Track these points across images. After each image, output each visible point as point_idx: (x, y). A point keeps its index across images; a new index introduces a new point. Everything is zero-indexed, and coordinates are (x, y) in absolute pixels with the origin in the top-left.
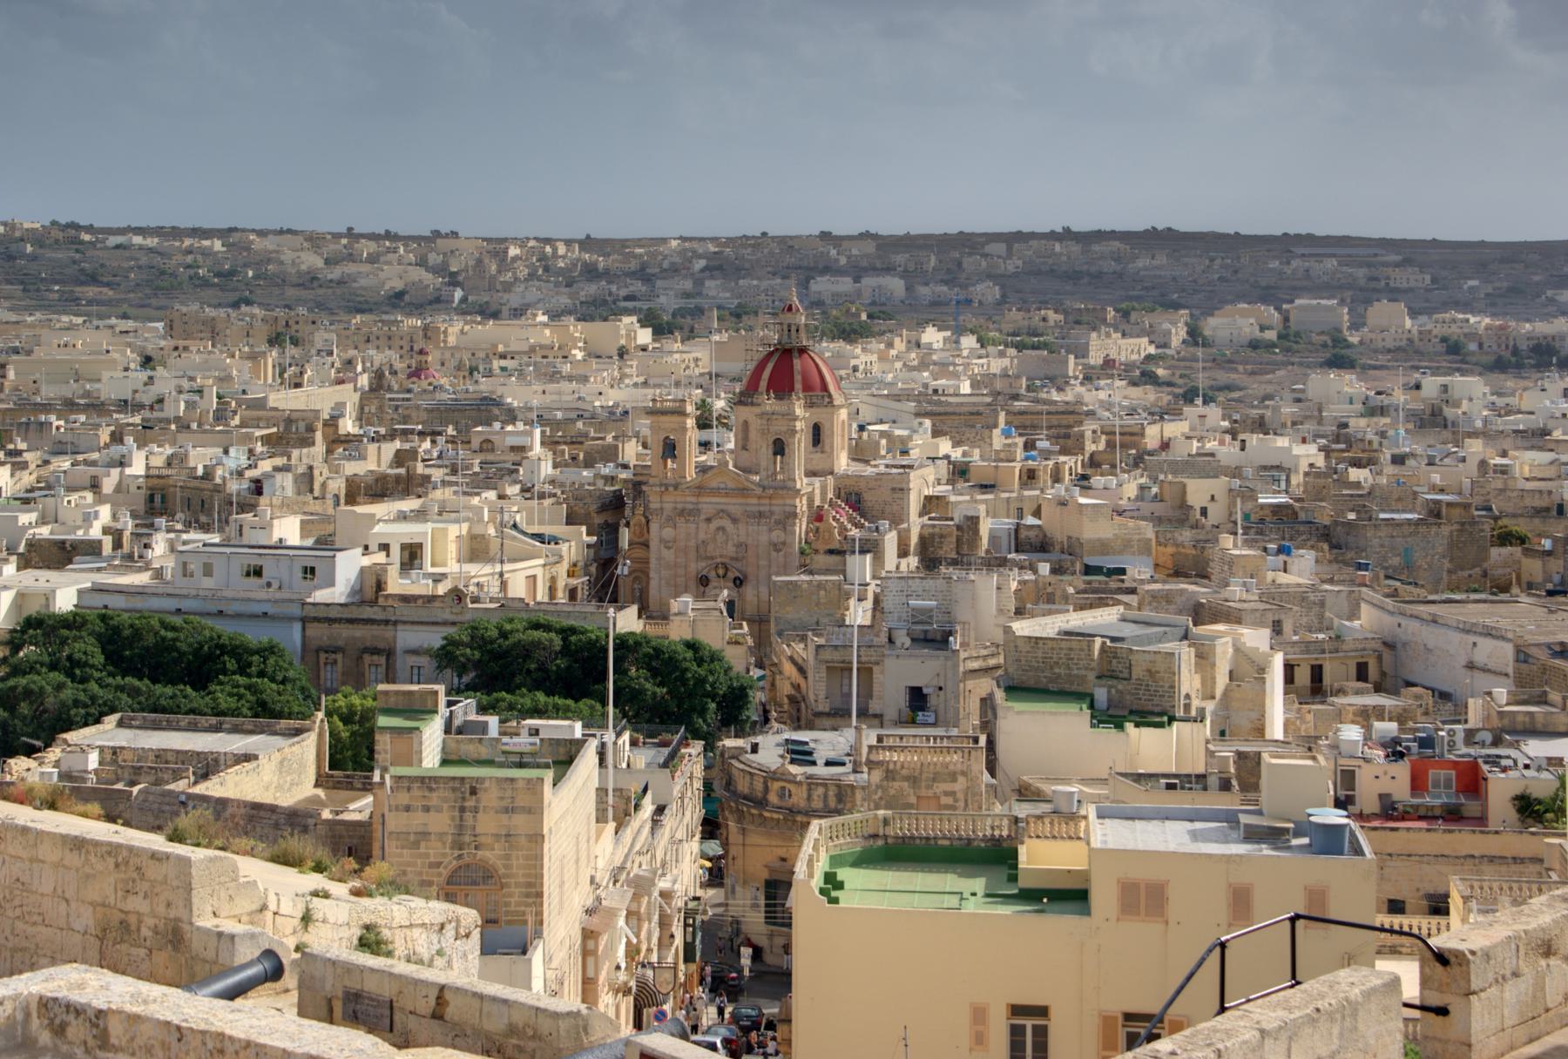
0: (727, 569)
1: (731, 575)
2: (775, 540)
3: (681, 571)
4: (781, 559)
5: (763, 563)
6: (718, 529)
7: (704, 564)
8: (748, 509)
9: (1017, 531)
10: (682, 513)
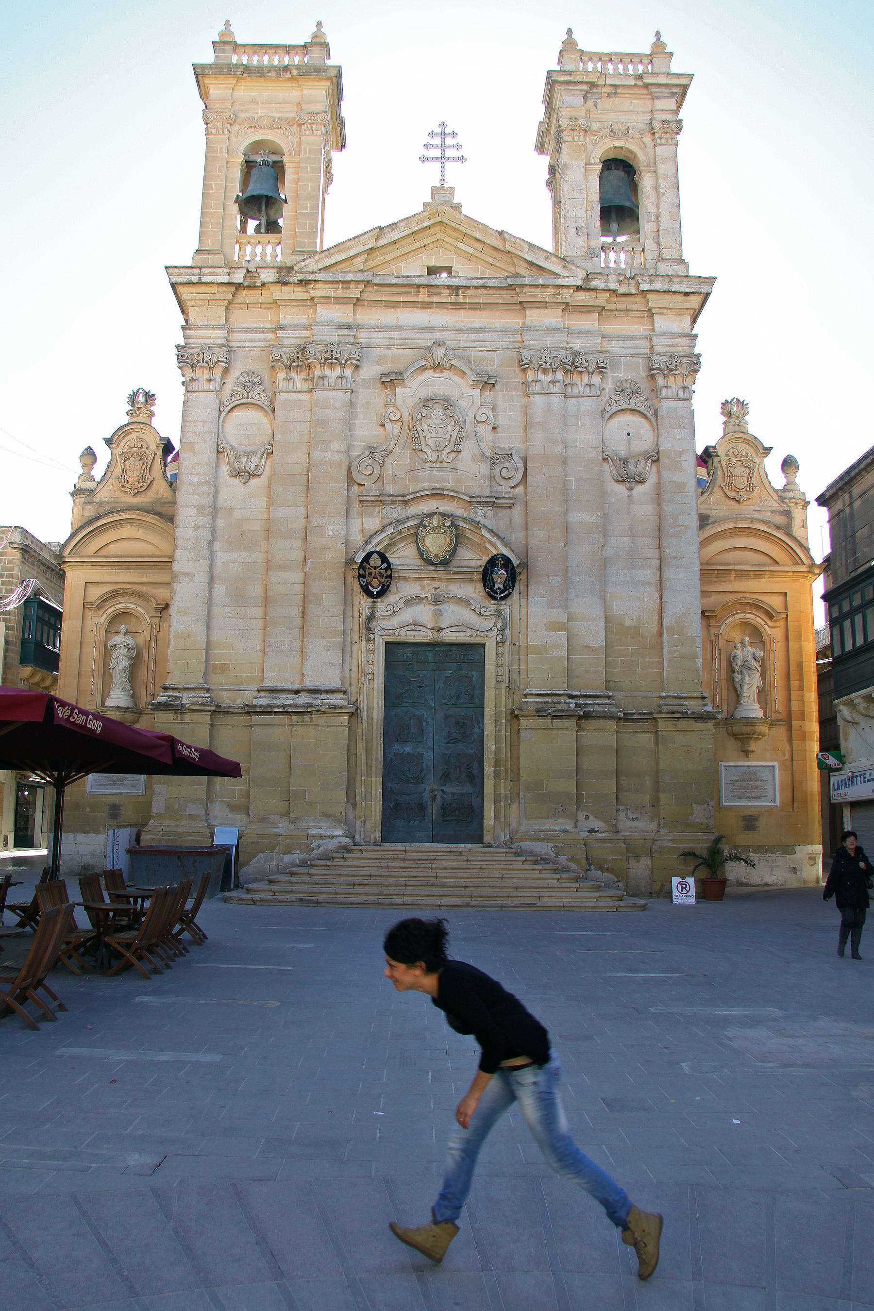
0: (458, 539)
3: (290, 550)
4: (645, 510)
5: (580, 517)
6: (427, 402)
7: (372, 523)
8: (530, 340)
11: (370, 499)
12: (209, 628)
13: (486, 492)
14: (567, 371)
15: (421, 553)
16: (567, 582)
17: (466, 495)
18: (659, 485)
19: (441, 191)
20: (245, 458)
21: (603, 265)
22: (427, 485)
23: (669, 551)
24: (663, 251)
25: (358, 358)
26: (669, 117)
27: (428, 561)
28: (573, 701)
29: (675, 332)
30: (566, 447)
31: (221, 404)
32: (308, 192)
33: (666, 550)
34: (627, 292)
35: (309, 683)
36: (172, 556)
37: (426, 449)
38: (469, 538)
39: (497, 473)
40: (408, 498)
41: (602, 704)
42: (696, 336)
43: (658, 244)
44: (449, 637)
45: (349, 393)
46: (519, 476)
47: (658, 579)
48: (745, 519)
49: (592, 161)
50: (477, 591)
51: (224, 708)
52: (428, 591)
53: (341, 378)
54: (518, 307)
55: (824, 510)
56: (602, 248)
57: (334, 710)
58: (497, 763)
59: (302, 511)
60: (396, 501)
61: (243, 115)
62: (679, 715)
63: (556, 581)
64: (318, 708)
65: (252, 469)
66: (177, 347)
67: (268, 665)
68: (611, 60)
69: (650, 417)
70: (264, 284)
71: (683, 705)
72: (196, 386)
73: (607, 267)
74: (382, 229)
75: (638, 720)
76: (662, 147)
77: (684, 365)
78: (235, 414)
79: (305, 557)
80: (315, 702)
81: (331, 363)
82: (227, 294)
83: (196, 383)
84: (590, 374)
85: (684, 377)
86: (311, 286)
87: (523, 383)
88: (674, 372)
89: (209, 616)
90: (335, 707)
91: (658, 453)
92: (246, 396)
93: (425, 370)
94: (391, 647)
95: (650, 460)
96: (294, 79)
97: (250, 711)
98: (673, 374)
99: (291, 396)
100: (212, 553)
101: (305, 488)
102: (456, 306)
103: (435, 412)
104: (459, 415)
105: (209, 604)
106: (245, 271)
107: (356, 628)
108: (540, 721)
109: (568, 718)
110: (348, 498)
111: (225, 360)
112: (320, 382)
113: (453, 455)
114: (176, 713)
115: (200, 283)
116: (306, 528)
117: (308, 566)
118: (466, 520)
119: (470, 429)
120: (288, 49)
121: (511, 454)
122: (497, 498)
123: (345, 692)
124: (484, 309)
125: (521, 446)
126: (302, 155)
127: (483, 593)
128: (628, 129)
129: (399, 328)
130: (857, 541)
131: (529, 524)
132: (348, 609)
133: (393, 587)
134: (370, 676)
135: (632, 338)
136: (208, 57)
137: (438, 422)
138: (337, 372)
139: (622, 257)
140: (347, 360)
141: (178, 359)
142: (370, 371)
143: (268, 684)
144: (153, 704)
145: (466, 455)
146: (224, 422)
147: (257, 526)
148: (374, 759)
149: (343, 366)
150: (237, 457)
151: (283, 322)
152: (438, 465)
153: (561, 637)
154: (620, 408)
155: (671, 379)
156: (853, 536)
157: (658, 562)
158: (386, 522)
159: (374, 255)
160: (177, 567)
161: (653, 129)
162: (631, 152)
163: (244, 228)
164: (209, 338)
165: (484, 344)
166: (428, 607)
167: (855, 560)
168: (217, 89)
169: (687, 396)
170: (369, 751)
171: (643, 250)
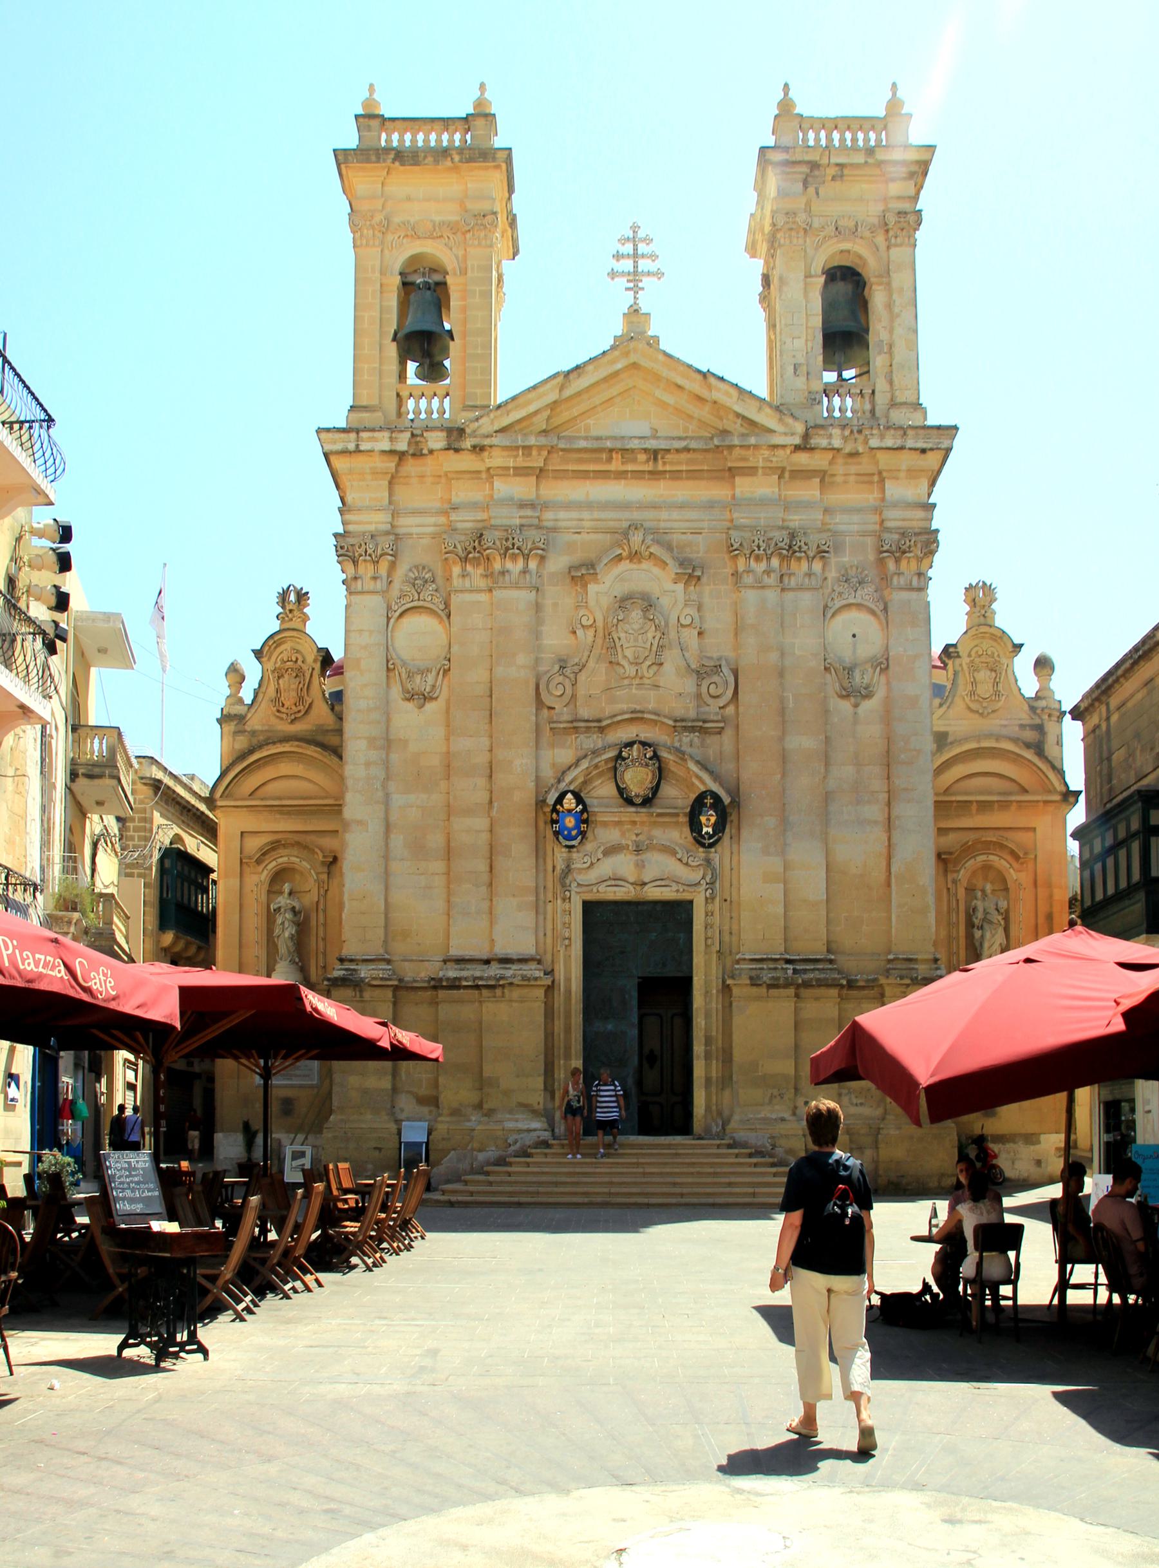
1: (676, 795)
2: (843, 649)
3: (472, 790)
4: (872, 731)
6: (624, 602)
7: (564, 755)
8: (742, 517)
11: (562, 726)
12: (387, 888)
13: (692, 714)
14: (782, 558)
15: (621, 791)
16: (784, 822)
17: (670, 718)
18: (888, 703)
19: (634, 314)
20: (419, 676)
21: (826, 414)
22: (625, 707)
23: (898, 782)
24: (897, 393)
25: (543, 546)
26: (906, 206)
27: (629, 801)
28: (791, 967)
29: (910, 501)
30: (783, 655)
31: (389, 608)
32: (479, 326)
33: (897, 782)
34: (854, 451)
35: (501, 950)
36: (340, 796)
37: (623, 662)
38: (673, 772)
39: (704, 690)
40: (604, 723)
41: (823, 969)
42: (934, 506)
43: (891, 383)
44: (654, 893)
45: (534, 592)
46: (730, 693)
47: (886, 816)
48: (989, 736)
49: (813, 273)
50: (683, 836)
51: (408, 982)
52: (629, 840)
53: (525, 571)
54: (727, 474)
55: (1078, 724)
56: (825, 392)
57: (528, 982)
58: (708, 1041)
59: (485, 742)
60: (590, 727)
61: (396, 220)
62: (908, 981)
63: (771, 821)
64: (510, 980)
65: (427, 690)
66: (336, 535)
67: (453, 930)
68: (836, 128)
69: (879, 612)
70: (431, 452)
71: (913, 969)
72: (359, 585)
73: (831, 416)
74: (568, 374)
75: (863, 988)
76: (898, 249)
77: (919, 545)
78: (406, 620)
79: (491, 799)
80: (509, 973)
81: (513, 554)
82: (391, 465)
83: (359, 582)
84: (810, 560)
85: (920, 560)
86: (486, 454)
87: (732, 575)
88: (907, 555)
89: (387, 873)
90: (529, 980)
91: (887, 660)
92: (417, 598)
93: (621, 560)
94: (589, 907)
95: (879, 668)
96: (455, 169)
97: (436, 985)
98: (906, 557)
99: (468, 597)
100: (387, 796)
101: (488, 713)
102: (655, 475)
103: (634, 614)
104: (661, 618)
105: (386, 858)
106: (408, 435)
107: (550, 885)
108: (755, 990)
109: (786, 986)
110: (537, 725)
111: (391, 552)
112: (501, 579)
113: (655, 668)
114: (355, 990)
115: (357, 451)
116: (491, 762)
117: (495, 809)
118: (669, 749)
119: (673, 634)
120: (446, 123)
121: (720, 666)
122: (705, 721)
123: (539, 962)
124: (688, 479)
125: (731, 654)
126: (469, 274)
127: (690, 838)
128: (856, 226)
129: (589, 506)
130: (1114, 764)
131: (741, 753)
132: (541, 861)
133: (589, 834)
134: (567, 942)
135: (858, 510)
136: (350, 139)
137: (636, 627)
138: (520, 564)
139: (849, 401)
140: (531, 550)
141: (337, 551)
142: (557, 563)
143: (454, 952)
144: (329, 979)
145: (668, 667)
146: (392, 632)
147: (436, 761)
148: (573, 1040)
149: (526, 557)
150: (410, 676)
151: (455, 500)
152: (637, 681)
153: (776, 891)
154: (845, 602)
155: (904, 563)
156: (1109, 759)
157: (886, 795)
158: (580, 753)
159: (558, 410)
160: (347, 813)
161: (886, 224)
162: (860, 257)
163: (402, 376)
164: (371, 523)
165: (687, 524)
166: (629, 857)
167: (1110, 790)
168: (366, 180)
169: (922, 584)
170: (568, 1030)
171: (873, 392)
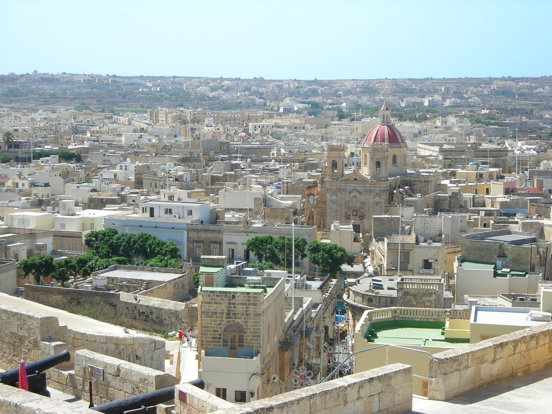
3: (339, 213)
8: (366, 188)
9: (473, 198)
10: (339, 190)
